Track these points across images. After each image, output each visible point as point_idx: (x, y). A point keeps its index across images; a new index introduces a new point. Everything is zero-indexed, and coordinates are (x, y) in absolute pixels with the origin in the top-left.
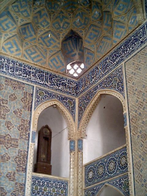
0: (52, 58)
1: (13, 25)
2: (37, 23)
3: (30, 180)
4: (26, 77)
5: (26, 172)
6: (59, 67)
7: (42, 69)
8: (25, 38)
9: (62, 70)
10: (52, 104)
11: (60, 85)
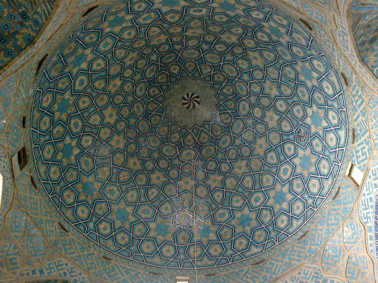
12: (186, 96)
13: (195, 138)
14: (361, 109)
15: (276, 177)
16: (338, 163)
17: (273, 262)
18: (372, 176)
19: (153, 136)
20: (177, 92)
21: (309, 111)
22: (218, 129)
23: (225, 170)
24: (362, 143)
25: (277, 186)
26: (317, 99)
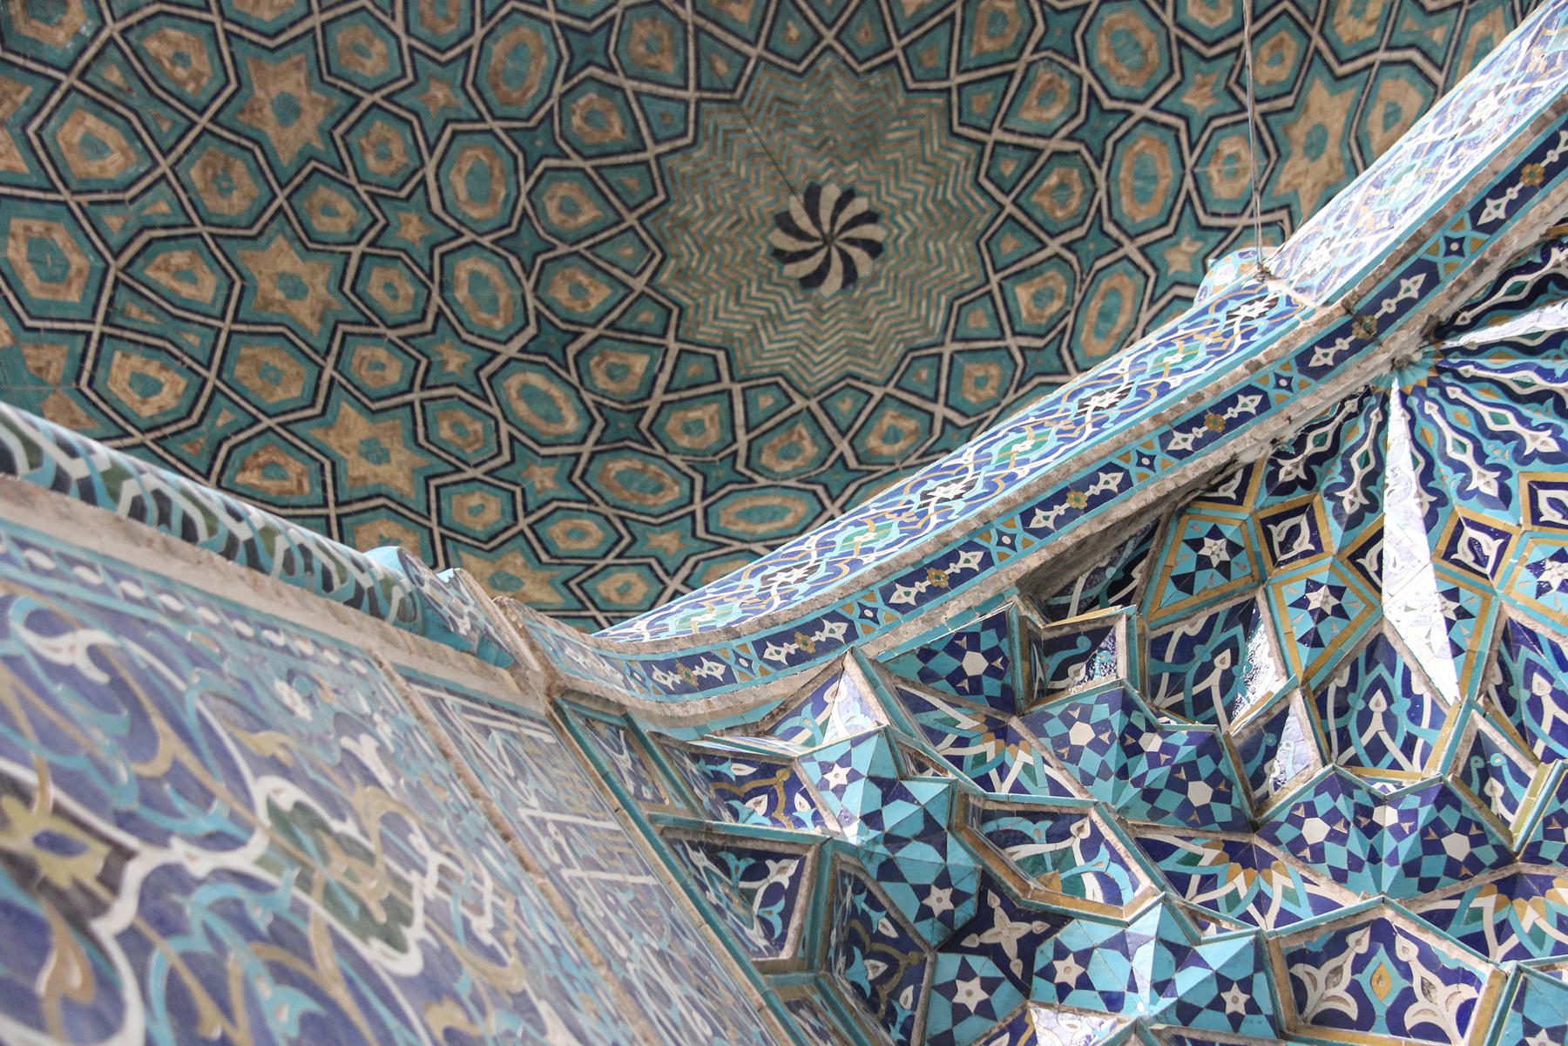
12: (831, 193)
13: (658, 391)
19: (509, 161)
20: (819, 127)
22: (800, 451)
23: (614, 597)
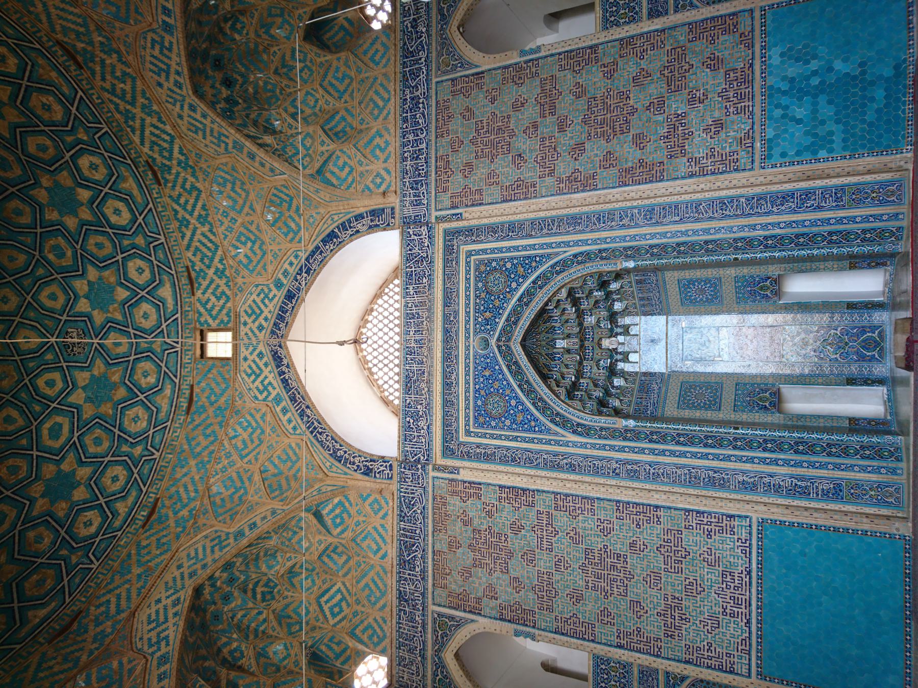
0: (372, 65)
1: (338, 157)
2: (315, 114)
3: (611, 31)
4: (423, 103)
5: (597, 45)
6: (383, 44)
7: (399, 76)
8: (352, 128)
9: (388, 37)
10: (460, 36)
11: (417, 32)
14: (196, 213)
15: (35, 453)
16: (174, 347)
17: (104, 599)
18: (246, 318)
21: (80, 286)
24: (212, 281)
25: (44, 468)
26: (95, 250)
